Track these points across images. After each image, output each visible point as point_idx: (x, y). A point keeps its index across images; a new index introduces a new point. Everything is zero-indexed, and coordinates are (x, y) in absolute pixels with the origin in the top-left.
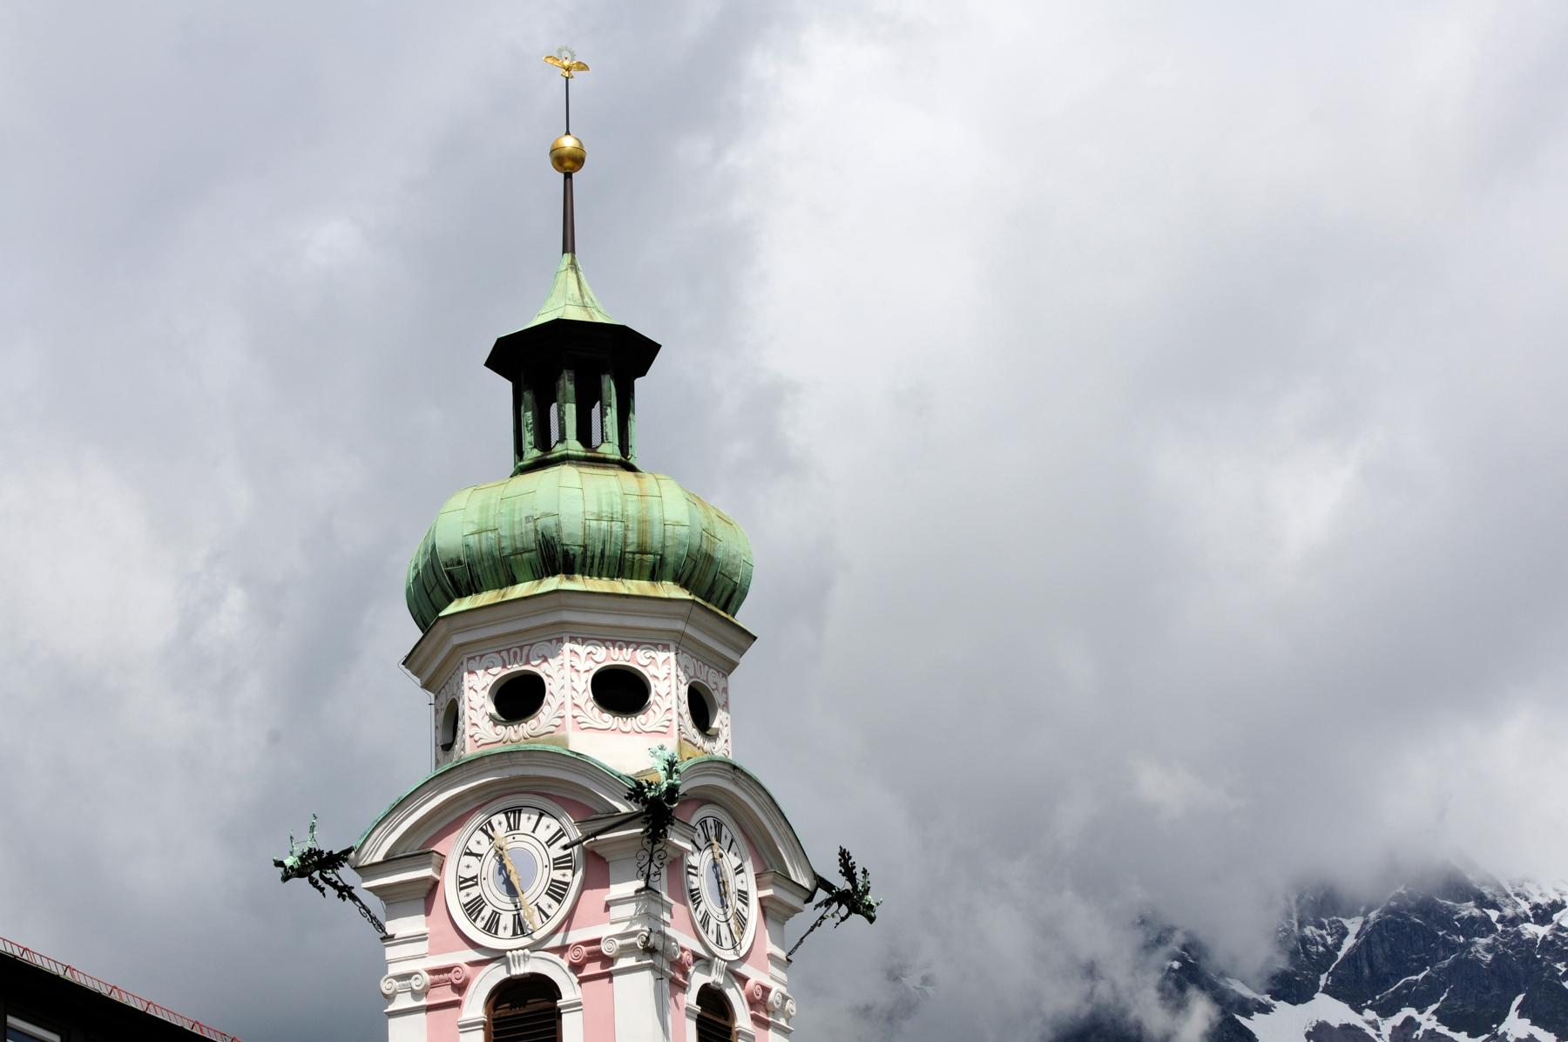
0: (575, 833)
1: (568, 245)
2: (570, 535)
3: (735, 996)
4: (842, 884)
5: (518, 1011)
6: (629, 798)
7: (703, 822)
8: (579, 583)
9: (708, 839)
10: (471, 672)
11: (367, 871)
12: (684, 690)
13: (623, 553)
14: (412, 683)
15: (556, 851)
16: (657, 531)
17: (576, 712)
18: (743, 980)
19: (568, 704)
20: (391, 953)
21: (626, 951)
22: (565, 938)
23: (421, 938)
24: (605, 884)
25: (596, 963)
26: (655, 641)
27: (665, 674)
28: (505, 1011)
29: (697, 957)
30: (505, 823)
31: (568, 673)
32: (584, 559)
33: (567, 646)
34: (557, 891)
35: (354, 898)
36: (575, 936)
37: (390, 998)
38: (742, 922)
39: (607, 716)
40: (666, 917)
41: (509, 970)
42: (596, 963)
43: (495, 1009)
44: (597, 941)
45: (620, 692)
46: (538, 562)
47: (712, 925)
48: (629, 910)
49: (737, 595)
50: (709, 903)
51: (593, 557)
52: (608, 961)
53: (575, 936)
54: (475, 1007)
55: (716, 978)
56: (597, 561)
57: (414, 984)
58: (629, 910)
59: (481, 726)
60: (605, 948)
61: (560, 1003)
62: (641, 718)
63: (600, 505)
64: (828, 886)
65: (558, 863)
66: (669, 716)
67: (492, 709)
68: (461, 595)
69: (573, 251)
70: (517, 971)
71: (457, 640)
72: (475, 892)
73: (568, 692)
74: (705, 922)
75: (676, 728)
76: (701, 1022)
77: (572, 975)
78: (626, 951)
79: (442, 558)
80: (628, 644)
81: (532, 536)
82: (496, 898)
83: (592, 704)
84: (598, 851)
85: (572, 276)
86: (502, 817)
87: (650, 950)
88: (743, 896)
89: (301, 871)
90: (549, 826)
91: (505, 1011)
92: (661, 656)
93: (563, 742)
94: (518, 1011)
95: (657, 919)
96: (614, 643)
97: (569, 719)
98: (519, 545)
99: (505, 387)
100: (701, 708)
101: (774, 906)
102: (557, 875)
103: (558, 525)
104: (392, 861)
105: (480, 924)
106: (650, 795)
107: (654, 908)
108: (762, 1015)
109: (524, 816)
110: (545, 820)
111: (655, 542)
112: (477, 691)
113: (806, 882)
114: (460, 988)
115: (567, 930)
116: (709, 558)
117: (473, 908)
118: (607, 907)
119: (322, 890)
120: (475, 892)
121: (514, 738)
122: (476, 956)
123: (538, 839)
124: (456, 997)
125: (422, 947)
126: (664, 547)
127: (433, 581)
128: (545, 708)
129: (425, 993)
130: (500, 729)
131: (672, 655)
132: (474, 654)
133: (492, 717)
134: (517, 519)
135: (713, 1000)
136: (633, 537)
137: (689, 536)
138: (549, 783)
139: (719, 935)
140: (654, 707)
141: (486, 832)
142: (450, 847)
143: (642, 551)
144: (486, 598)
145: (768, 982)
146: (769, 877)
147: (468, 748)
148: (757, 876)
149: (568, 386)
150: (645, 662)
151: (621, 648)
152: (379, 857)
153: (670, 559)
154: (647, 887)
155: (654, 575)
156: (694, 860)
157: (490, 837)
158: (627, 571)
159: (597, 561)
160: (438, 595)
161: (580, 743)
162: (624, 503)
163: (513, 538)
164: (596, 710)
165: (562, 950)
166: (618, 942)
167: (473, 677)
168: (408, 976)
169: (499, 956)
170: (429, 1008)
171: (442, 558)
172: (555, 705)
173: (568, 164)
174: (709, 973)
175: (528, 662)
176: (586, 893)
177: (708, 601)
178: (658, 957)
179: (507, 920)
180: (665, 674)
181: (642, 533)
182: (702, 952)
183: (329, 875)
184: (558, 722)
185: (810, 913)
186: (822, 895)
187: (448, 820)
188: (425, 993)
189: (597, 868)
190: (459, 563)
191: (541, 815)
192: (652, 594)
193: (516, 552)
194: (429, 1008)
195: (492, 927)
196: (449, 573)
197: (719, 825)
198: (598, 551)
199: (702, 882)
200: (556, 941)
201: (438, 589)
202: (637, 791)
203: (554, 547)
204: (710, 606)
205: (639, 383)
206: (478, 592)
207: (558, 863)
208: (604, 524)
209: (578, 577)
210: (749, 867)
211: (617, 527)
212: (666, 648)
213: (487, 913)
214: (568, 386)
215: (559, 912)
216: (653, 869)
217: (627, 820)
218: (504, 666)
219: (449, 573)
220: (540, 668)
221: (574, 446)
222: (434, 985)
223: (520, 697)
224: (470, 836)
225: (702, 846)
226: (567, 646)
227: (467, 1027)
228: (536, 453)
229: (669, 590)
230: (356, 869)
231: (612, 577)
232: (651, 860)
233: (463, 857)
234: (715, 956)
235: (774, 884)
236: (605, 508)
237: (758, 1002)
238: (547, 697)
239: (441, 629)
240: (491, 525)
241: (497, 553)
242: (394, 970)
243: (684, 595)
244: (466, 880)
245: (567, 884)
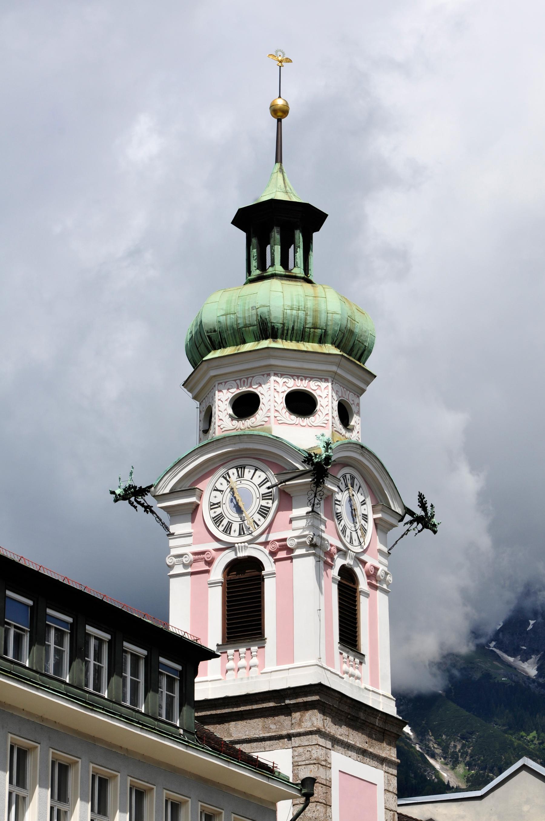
0: (274, 480)
1: (279, 159)
2: (275, 317)
3: (359, 572)
4: (419, 512)
5: (241, 576)
6: (304, 462)
7: (344, 476)
8: (280, 344)
9: (347, 486)
10: (220, 391)
11: (160, 498)
12: (336, 404)
13: (304, 328)
14: (187, 396)
15: (264, 490)
16: (323, 317)
17: (277, 414)
18: (364, 563)
19: (272, 410)
20: (172, 543)
21: (300, 545)
22: (267, 537)
23: (189, 535)
24: (290, 508)
25: (284, 551)
26: (321, 377)
27: (325, 395)
28: (234, 576)
29: (339, 550)
31: (273, 393)
32: (283, 331)
33: (273, 378)
34: (263, 512)
35: (153, 512)
36: (273, 537)
37: (171, 567)
38: (364, 530)
39: (293, 417)
40: (323, 527)
41: (236, 554)
42: (284, 551)
43: (228, 575)
44: (285, 540)
45: (301, 404)
46: (258, 333)
47: (348, 533)
48: (303, 523)
49: (366, 352)
50: (346, 520)
51: (288, 330)
52: (290, 550)
53: (273, 537)
54: (217, 574)
55: (349, 561)
56: (290, 332)
57: (185, 560)
58: (303, 523)
59: (224, 421)
60: (289, 544)
61: (263, 573)
62: (312, 418)
63: (292, 301)
64: (412, 513)
65: (265, 497)
66: (327, 418)
67: (231, 411)
68: (215, 349)
69: (281, 162)
70: (241, 554)
71: (213, 373)
72: (219, 511)
73: (272, 403)
74: (344, 531)
75: (331, 424)
76: (341, 586)
77: (270, 558)
78: (300, 545)
79: (205, 328)
80: (306, 378)
81: (255, 317)
82: (231, 515)
83: (285, 410)
84: (287, 491)
85: (280, 175)
86: (234, 470)
87: (313, 545)
88: (365, 517)
89: (125, 497)
90: (260, 476)
91: (234, 576)
92: (323, 385)
93: (269, 430)
94: (241, 576)
95: (318, 528)
96: (298, 377)
97: (272, 418)
98: (248, 322)
99: (242, 235)
100: (345, 414)
101: (383, 523)
102: (264, 503)
103: (269, 312)
104: (174, 493)
105: (221, 528)
106: (315, 461)
107: (316, 522)
108: (374, 582)
109: (246, 470)
110: (258, 473)
111: (322, 322)
112: (223, 401)
113: (400, 511)
114: (209, 563)
115: (269, 533)
116: (351, 332)
117: (218, 520)
118: (291, 521)
119: (135, 507)
120: (219, 511)
121: (242, 428)
122: (218, 546)
123: (254, 483)
124: (207, 568)
125: (189, 540)
126: (327, 325)
127: (200, 341)
128: (259, 412)
129: (190, 565)
130: (235, 422)
131: (330, 384)
132: (222, 381)
133: (230, 416)
134: (247, 308)
135: (347, 574)
136: (310, 320)
137: (341, 320)
138: (260, 453)
139: (351, 538)
140: (319, 413)
141: (225, 478)
142: (206, 486)
143: (315, 328)
144: (229, 351)
145: (377, 565)
146: (380, 507)
147: (217, 432)
148: (373, 507)
149: (276, 236)
150: (315, 388)
151: (302, 380)
152: (167, 491)
153: (330, 332)
154: (313, 511)
155: (321, 341)
156: (339, 497)
157: (228, 481)
158: (306, 338)
159: (290, 332)
160: (202, 348)
161: (278, 431)
162: (306, 301)
163: (244, 318)
164: (287, 414)
165: (265, 544)
166: (296, 540)
167: (221, 393)
168: (181, 556)
169: (231, 546)
170: (193, 574)
171: (205, 328)
172: (265, 410)
173: (279, 113)
174: (346, 559)
175: (251, 386)
176: (279, 513)
177: (350, 355)
178: (318, 549)
179: (236, 527)
180: (325, 395)
181: (315, 317)
182: (342, 547)
183: (140, 499)
184: (267, 419)
185: (401, 528)
186: (408, 518)
187: (205, 471)
188: (190, 565)
189: (286, 499)
190: (215, 331)
191: (256, 470)
192: (319, 350)
193: (246, 326)
194: (193, 574)
195: (227, 530)
196: (209, 336)
197: (353, 478)
198: (291, 327)
199: (343, 509)
200: (262, 539)
201: (202, 346)
202: (309, 459)
203: (266, 324)
204: (351, 358)
205: (315, 235)
206: (224, 347)
207: (265, 497)
208: (294, 312)
209: (279, 340)
210: (369, 501)
211: (301, 314)
212: (326, 380)
213: (225, 522)
214: (276, 236)
215: (264, 523)
216: (316, 501)
217: (303, 474)
218: (238, 388)
219: (209, 336)
220: (258, 390)
221: (279, 269)
222: (195, 561)
223: (246, 405)
224: (217, 480)
225: (343, 489)
226: (273, 378)
227: (212, 584)
228: (258, 272)
229: (330, 349)
230: (154, 496)
231: (298, 341)
232: (315, 496)
233: (213, 491)
234: (349, 549)
235: (382, 511)
236: (295, 303)
237: (372, 575)
238: (261, 405)
239: (204, 367)
240: (232, 311)
241: (235, 326)
242: (174, 552)
243: (337, 351)
244: (214, 504)
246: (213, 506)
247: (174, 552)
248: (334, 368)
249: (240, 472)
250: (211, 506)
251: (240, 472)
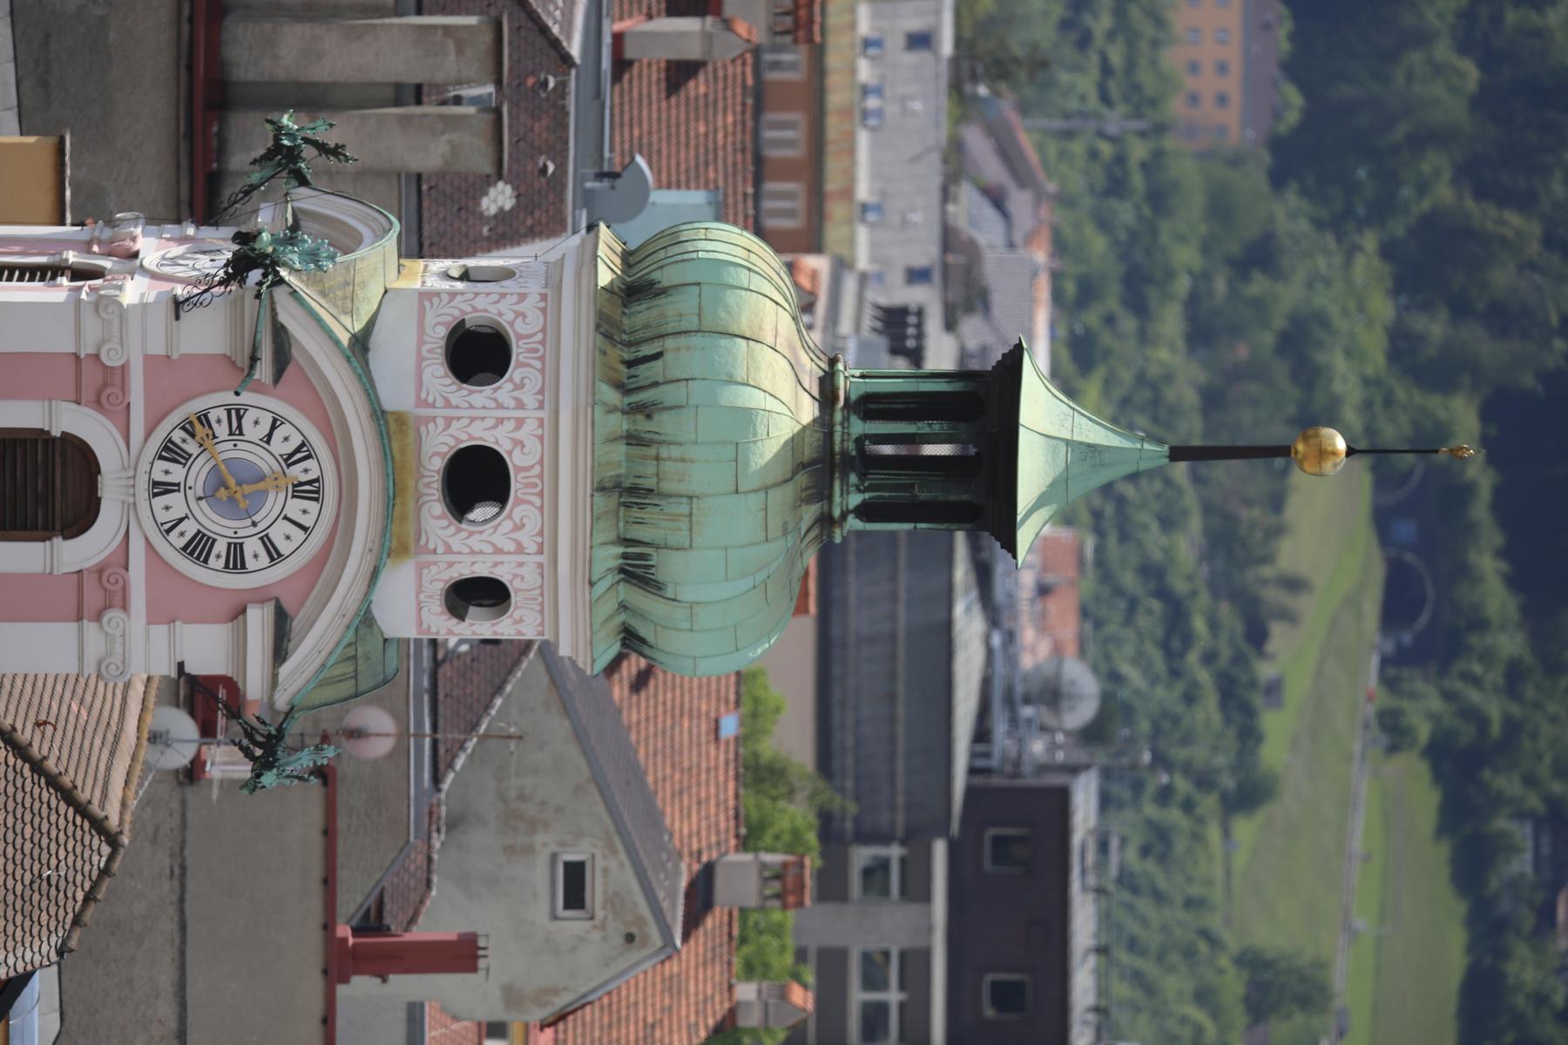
30: (304, 478)
72: (222, 431)
120: (222, 431)
141: (298, 450)
244: (239, 418)
245: (206, 561)
246: (236, 414)
249: (307, 488)
250: (238, 411)
251: (307, 488)
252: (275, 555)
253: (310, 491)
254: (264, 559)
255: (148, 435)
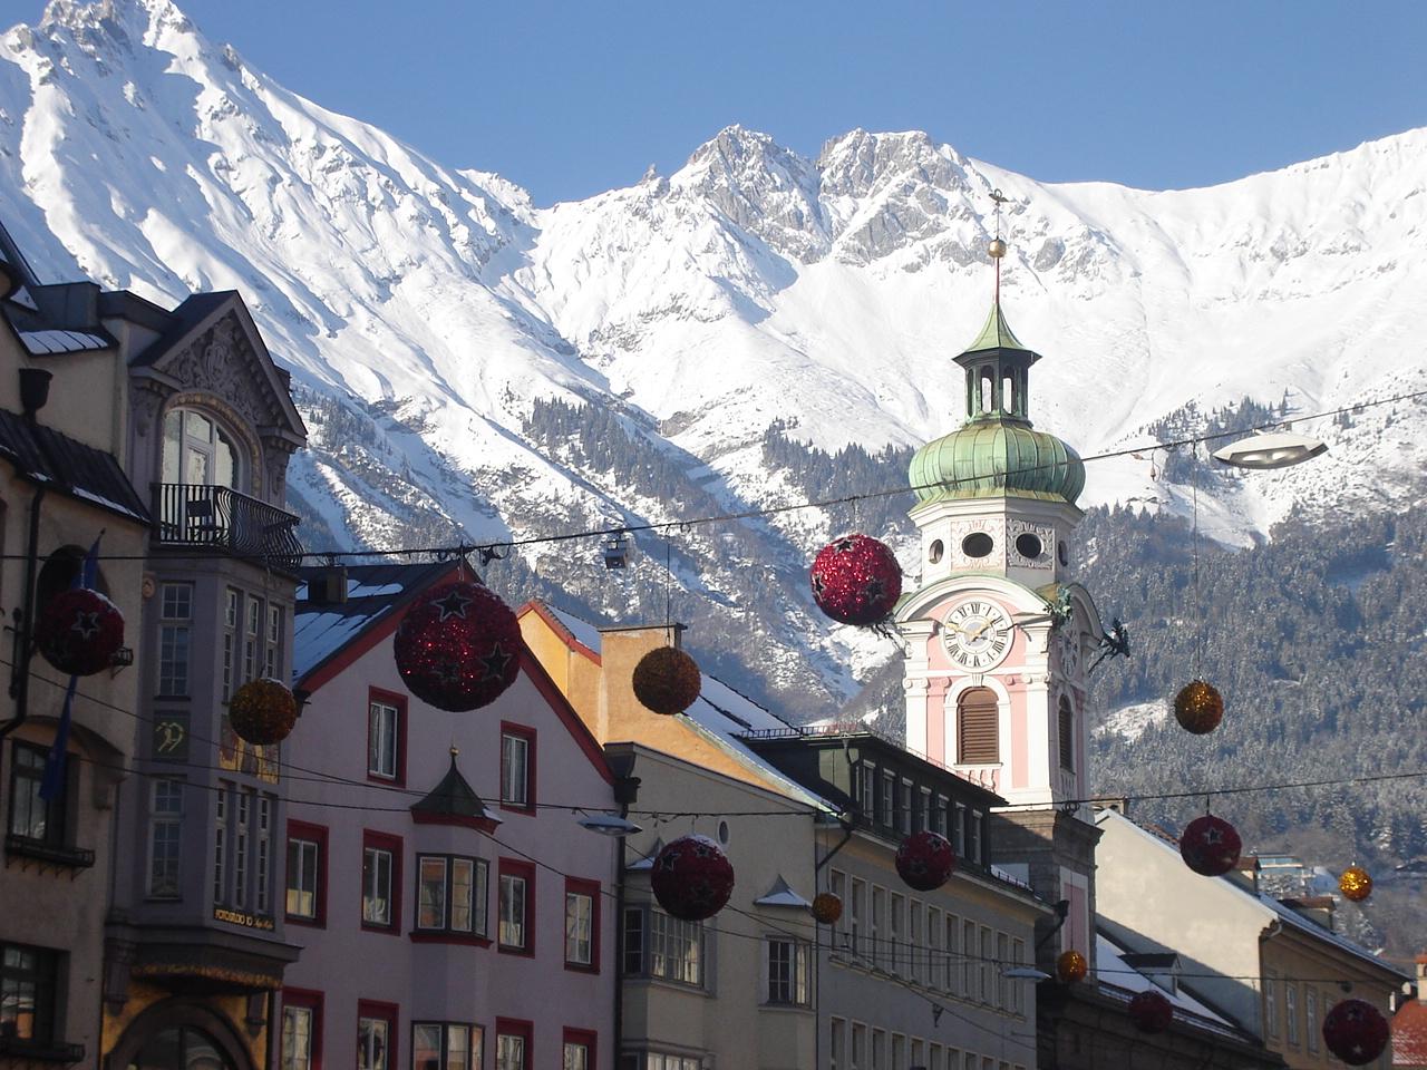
39: (1023, 558)
72: (954, 642)
99: (962, 372)
105: (957, 658)
117: (953, 650)
120: (954, 642)
135: (1065, 701)
179: (971, 658)
195: (963, 660)
213: (960, 653)
247: (909, 675)
248: (1059, 515)
252: (1001, 618)
253: (976, 608)
254: (1002, 622)
255: (954, 669)
